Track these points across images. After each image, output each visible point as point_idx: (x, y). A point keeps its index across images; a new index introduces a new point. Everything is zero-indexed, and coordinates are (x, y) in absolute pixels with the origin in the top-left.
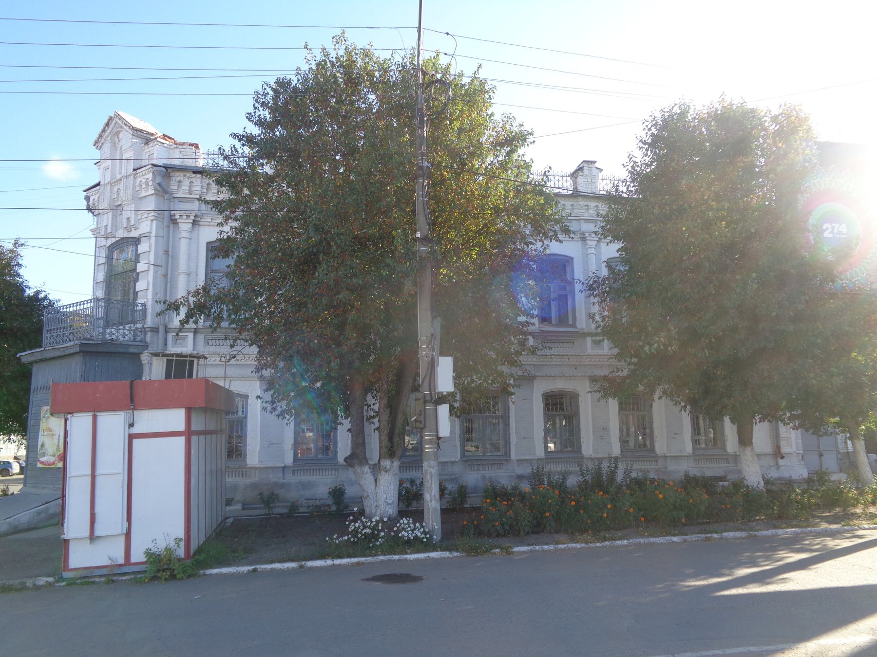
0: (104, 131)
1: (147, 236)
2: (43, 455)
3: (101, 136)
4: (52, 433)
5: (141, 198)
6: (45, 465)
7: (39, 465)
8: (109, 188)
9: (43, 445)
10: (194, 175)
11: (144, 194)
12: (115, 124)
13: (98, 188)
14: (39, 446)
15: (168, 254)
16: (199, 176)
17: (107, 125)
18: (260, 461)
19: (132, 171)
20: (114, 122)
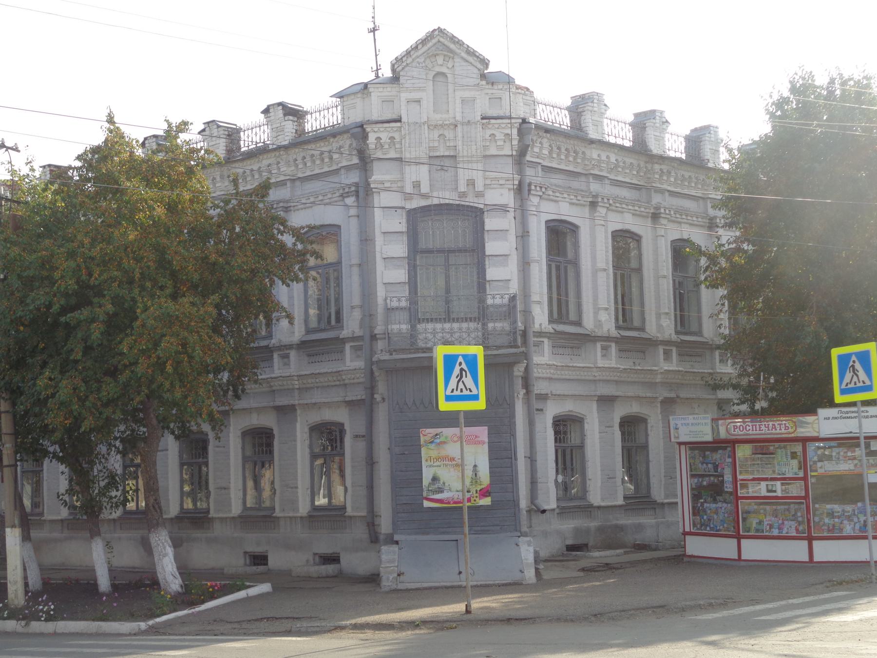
0: (415, 48)
1: (503, 209)
2: (440, 491)
3: (408, 53)
4: (454, 462)
5: (485, 157)
6: (449, 503)
7: (427, 504)
8: (426, 132)
9: (435, 479)
10: (545, 134)
11: (493, 151)
12: (435, 44)
13: (398, 124)
14: (426, 480)
15: (523, 236)
16: (548, 135)
17: (424, 42)
18: (603, 499)
19: (479, 118)
20: (434, 41)
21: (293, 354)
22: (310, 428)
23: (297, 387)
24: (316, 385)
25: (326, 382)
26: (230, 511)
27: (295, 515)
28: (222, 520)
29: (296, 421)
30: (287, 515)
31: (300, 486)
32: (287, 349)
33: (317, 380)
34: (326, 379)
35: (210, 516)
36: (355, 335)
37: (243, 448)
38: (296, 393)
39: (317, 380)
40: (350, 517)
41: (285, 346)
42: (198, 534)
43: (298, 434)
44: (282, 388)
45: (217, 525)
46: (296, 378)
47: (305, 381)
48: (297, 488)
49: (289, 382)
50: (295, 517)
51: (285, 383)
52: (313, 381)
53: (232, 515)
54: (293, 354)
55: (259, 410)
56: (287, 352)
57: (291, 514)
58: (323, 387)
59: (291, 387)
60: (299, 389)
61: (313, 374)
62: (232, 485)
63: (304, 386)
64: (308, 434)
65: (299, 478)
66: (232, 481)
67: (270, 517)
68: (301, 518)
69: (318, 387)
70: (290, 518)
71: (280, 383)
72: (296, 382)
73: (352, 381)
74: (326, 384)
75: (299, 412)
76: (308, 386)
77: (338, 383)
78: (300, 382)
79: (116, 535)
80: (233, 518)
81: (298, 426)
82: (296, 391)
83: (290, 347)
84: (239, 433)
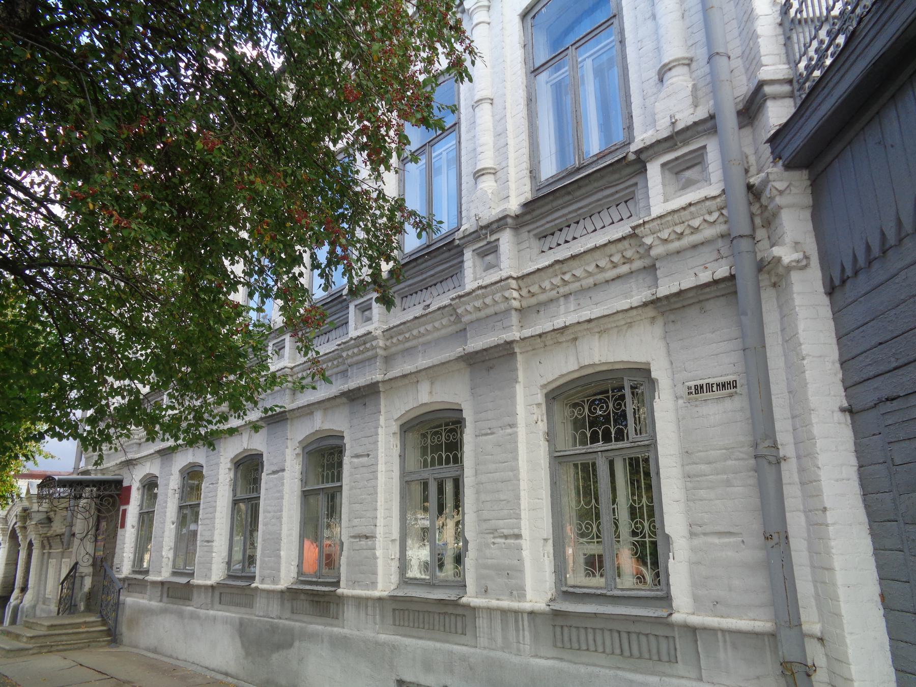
21: (506, 239)
22: (547, 395)
23: (516, 304)
24: (562, 290)
25: (590, 274)
26: (374, 584)
27: (515, 605)
28: (361, 601)
29: (516, 381)
30: (494, 603)
31: (525, 532)
32: (492, 232)
33: (567, 277)
34: (591, 268)
35: (339, 591)
36: (680, 126)
37: (402, 457)
38: (514, 317)
39: (567, 277)
40: (692, 631)
41: (487, 226)
42: (317, 627)
43: (520, 409)
44: (482, 314)
45: (350, 613)
46: (513, 284)
47: (535, 289)
48: (518, 536)
49: (498, 297)
50: (516, 612)
51: (488, 300)
52: (557, 281)
53: (377, 593)
54: (506, 239)
55: (432, 373)
56: (494, 238)
57: (505, 604)
58: (583, 290)
59: (503, 306)
60: (519, 310)
61: (557, 262)
62: (380, 531)
63: (533, 301)
64: (544, 407)
65: (524, 515)
66: (380, 522)
67: (455, 604)
68: (532, 613)
69: (566, 296)
70: (504, 612)
71: (478, 304)
72: (515, 294)
73: (676, 245)
74: (590, 281)
75: (519, 358)
76: (543, 297)
77: (625, 269)
78: (524, 292)
79: (211, 612)
80: (380, 599)
81: (519, 389)
82: (513, 312)
83: (500, 223)
84: (395, 428)
